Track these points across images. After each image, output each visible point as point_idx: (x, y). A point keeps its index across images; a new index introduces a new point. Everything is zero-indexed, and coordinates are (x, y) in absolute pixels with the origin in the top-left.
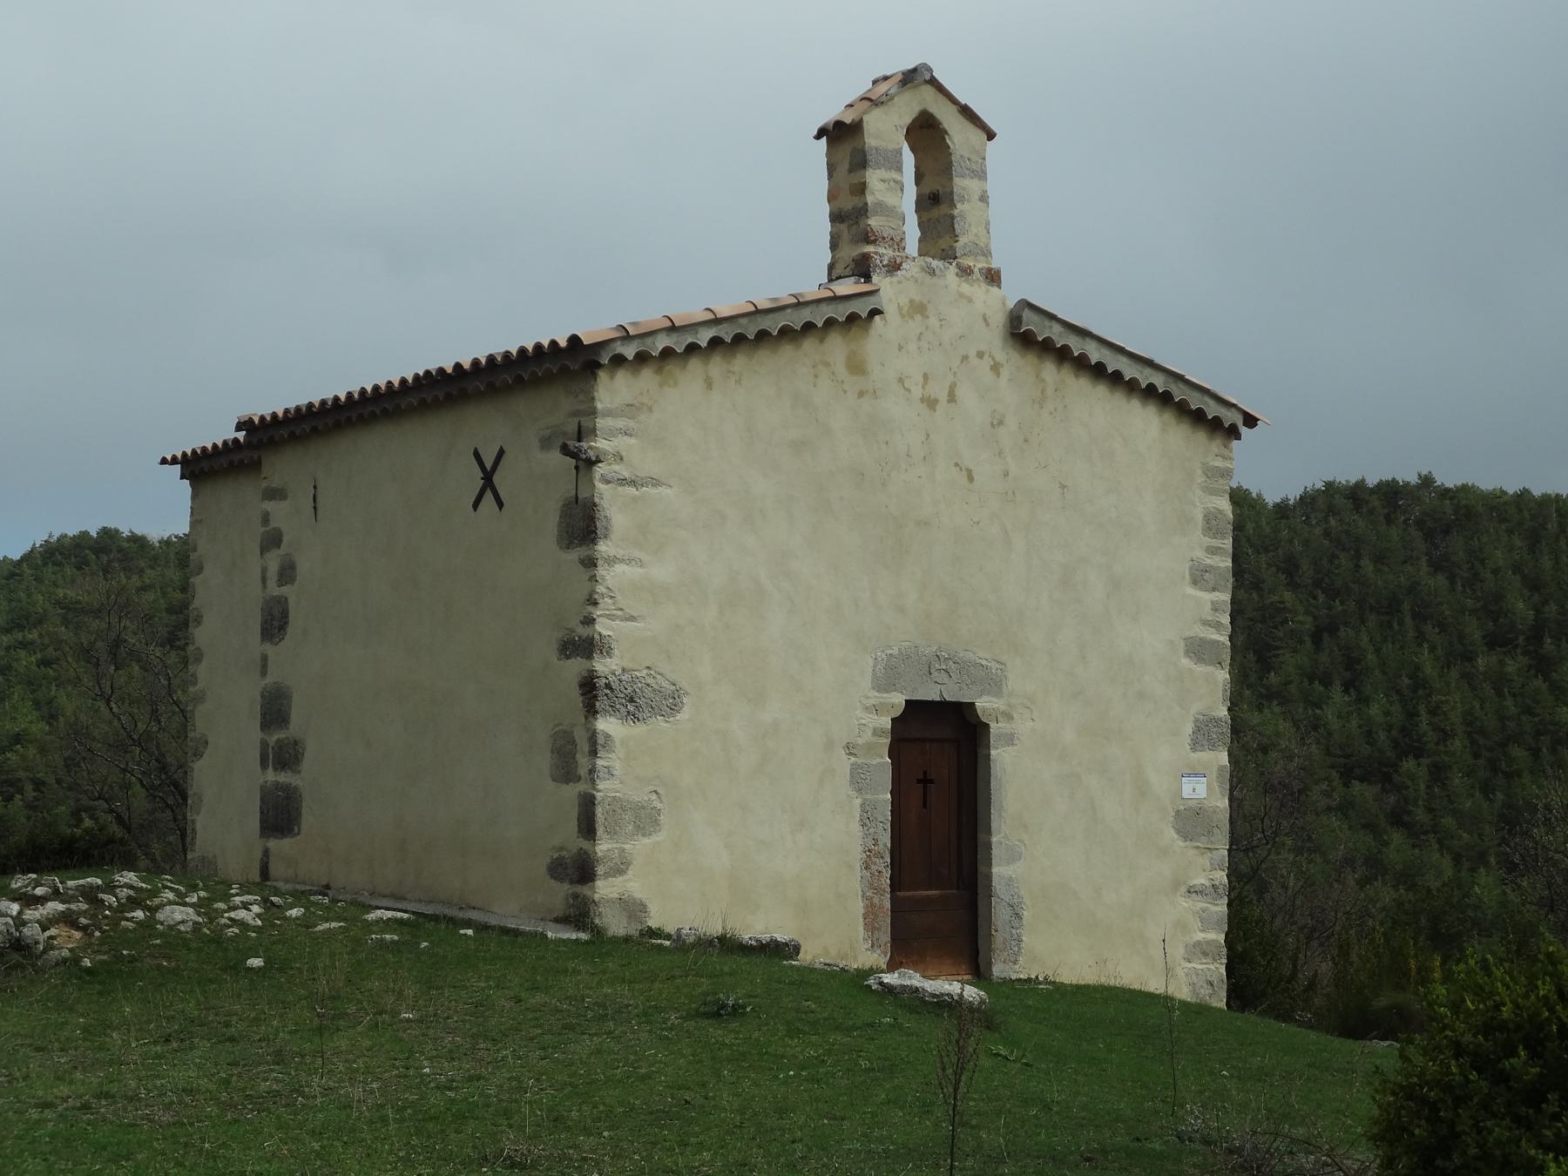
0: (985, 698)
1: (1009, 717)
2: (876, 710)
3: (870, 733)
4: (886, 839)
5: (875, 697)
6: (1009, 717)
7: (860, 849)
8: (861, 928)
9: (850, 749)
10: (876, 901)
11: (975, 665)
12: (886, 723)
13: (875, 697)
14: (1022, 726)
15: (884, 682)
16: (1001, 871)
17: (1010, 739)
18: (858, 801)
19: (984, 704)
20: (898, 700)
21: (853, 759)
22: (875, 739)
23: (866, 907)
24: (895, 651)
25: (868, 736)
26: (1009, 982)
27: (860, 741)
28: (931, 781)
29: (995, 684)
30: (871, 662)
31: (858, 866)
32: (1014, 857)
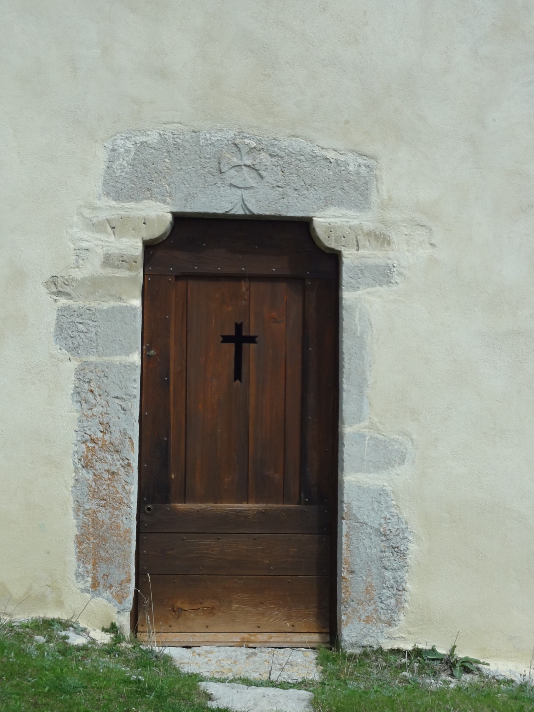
0: (332, 211)
1: (382, 240)
2: (113, 227)
3: (97, 261)
4: (128, 424)
5: (110, 208)
6: (382, 240)
7: (73, 437)
8: (72, 558)
9: (58, 286)
10: (104, 516)
11: (313, 159)
12: (135, 248)
13: (110, 208)
14: (408, 254)
15: (130, 180)
16: (356, 480)
17: (384, 275)
18: (74, 365)
19: (330, 222)
20: (157, 215)
21: (63, 301)
22: (109, 272)
23: (82, 526)
24: (153, 138)
25: (93, 267)
26: (370, 655)
27: (78, 274)
28: (252, 340)
29: (356, 189)
30: (103, 155)
31: (69, 463)
32: (388, 456)
